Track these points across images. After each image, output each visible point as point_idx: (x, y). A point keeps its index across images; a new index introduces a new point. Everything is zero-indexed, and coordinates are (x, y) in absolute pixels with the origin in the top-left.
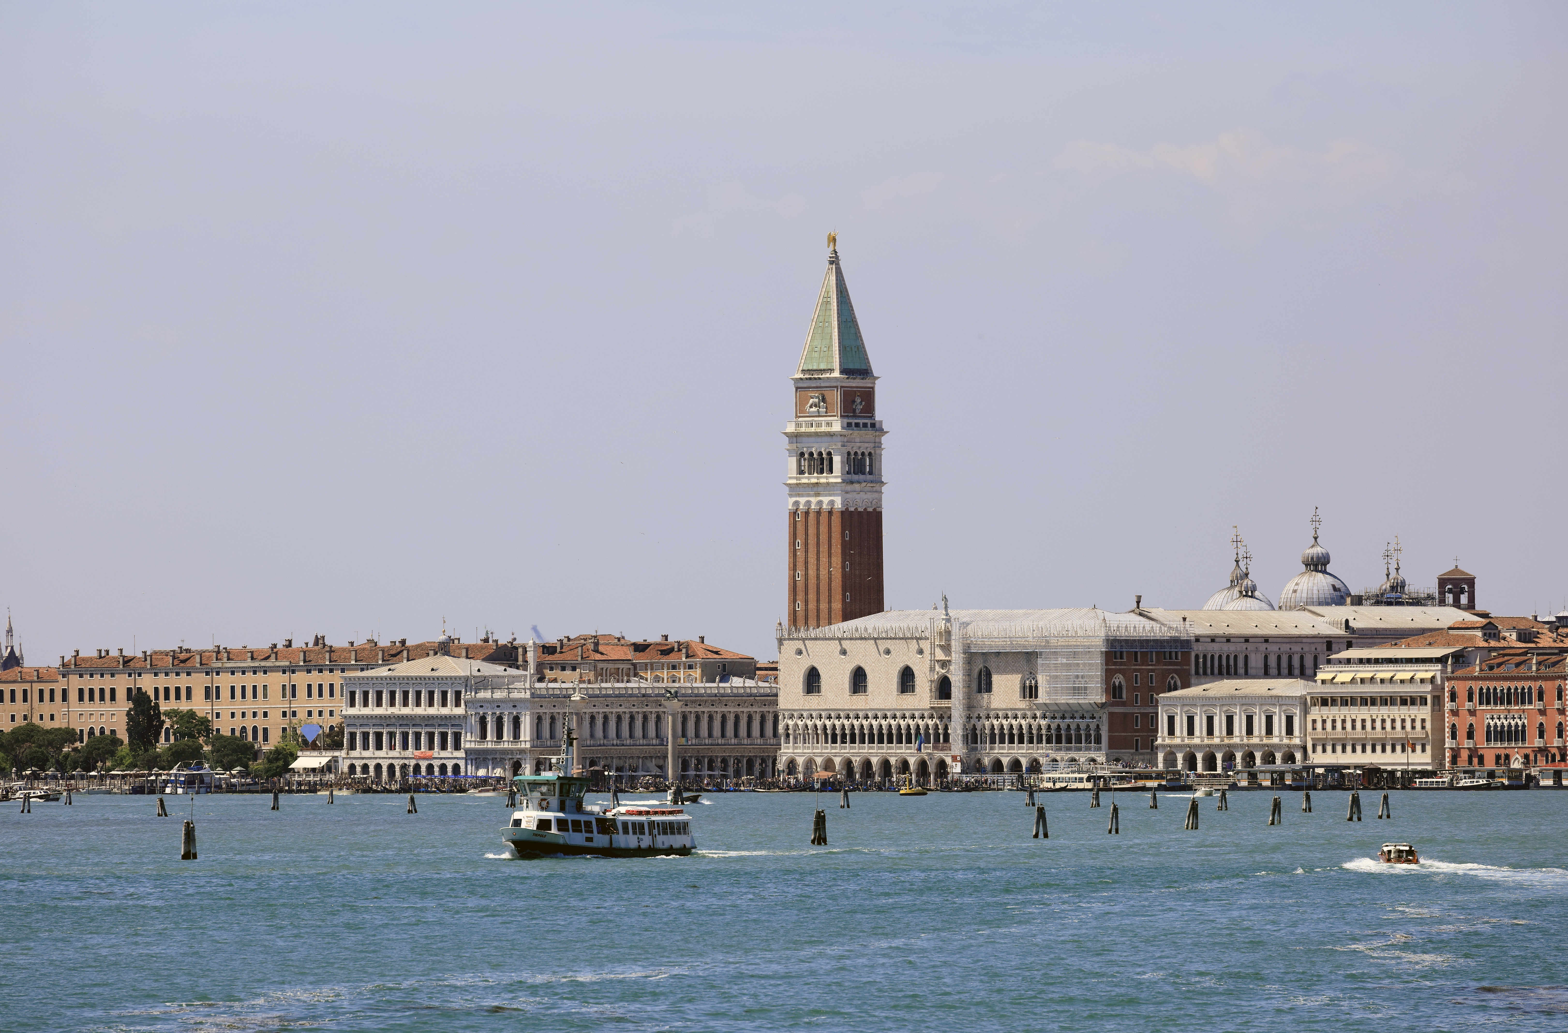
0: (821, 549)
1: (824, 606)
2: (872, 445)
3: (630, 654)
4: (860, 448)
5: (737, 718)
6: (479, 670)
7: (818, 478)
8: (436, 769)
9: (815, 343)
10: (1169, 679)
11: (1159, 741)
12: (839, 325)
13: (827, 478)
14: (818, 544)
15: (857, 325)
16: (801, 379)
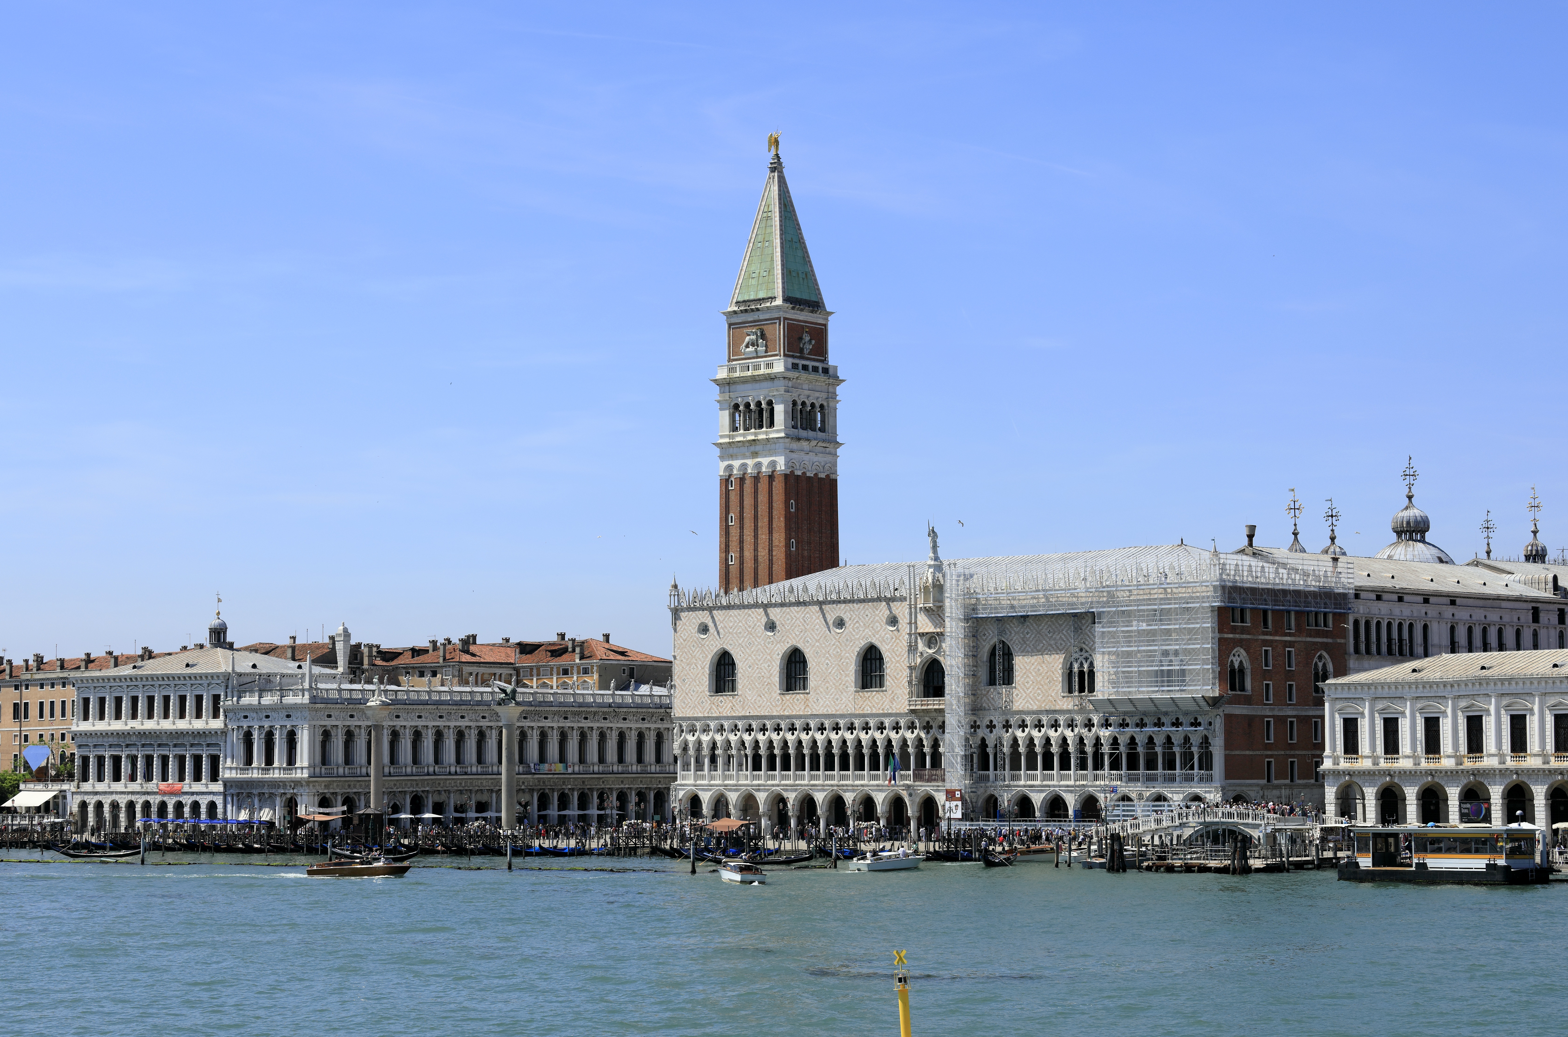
0: (759, 524)
2: (824, 395)
3: (513, 656)
4: (808, 397)
5: (641, 736)
6: (254, 666)
7: (756, 434)
8: (187, 810)
9: (753, 268)
10: (1316, 660)
11: (1327, 764)
12: (782, 243)
13: (766, 433)
15: (805, 247)
16: (735, 312)
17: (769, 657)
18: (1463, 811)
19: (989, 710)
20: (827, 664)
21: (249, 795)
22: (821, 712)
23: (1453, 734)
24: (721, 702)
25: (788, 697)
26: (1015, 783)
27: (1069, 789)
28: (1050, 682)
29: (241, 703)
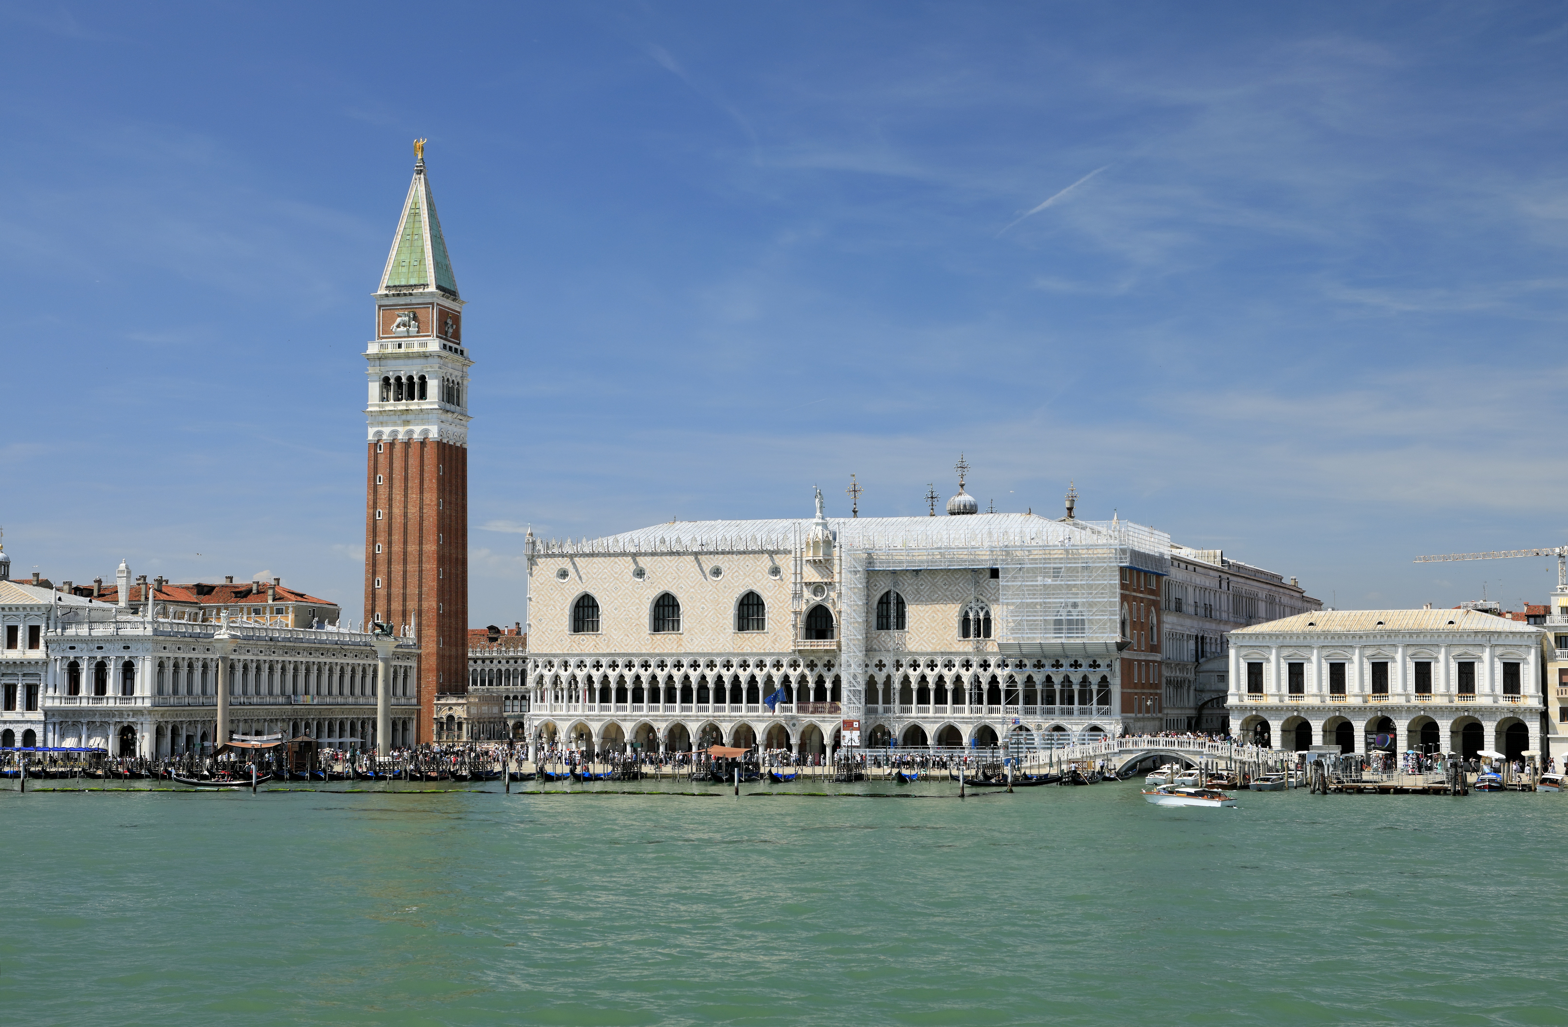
0: (409, 485)
1: (412, 548)
2: (460, 374)
7: (407, 405)
11: (1232, 701)
14: (406, 479)
16: (387, 295)
17: (637, 601)
18: (1369, 740)
19: (880, 651)
20: (703, 608)
21: (75, 724)
22: (695, 651)
23: (1316, 677)
24: (583, 640)
25: (659, 637)
26: (906, 715)
27: (965, 721)
28: (945, 628)
29: (65, 634)
